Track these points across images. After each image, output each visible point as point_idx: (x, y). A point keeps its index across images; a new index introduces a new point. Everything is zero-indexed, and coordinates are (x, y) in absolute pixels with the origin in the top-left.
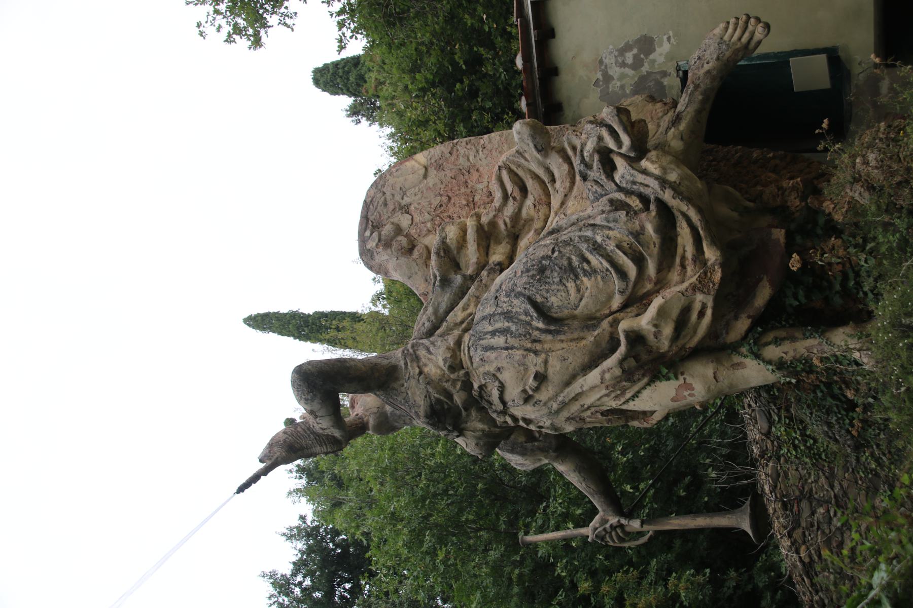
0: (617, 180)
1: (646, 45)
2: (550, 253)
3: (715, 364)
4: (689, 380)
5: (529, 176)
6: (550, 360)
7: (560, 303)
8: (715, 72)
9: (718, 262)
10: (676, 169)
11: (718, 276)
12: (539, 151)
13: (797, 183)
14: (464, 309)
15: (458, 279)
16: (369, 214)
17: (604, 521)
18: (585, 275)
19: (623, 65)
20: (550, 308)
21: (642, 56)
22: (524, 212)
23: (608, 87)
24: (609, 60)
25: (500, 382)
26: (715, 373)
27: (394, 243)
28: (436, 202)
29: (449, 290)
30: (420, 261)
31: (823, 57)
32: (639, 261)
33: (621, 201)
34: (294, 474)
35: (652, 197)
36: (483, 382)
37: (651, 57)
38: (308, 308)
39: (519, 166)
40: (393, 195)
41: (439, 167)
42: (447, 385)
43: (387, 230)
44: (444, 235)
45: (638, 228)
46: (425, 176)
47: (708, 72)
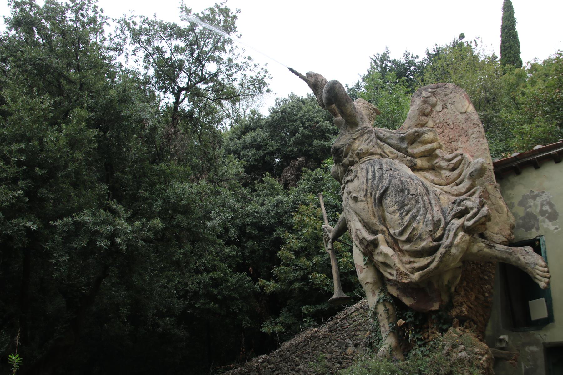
0: (453, 221)
1: (553, 217)
2: (411, 193)
3: (373, 282)
4: (364, 271)
5: (460, 171)
6: (363, 203)
7: (387, 203)
8: (519, 263)
9: (412, 280)
10: (458, 252)
11: (405, 281)
12: (470, 174)
13: (464, 312)
14: (391, 152)
15: (404, 145)
16: (440, 88)
17: (330, 231)
18: (400, 214)
19: (542, 205)
20: (385, 198)
21: (547, 215)
23: (530, 199)
24: (544, 197)
25: (354, 179)
26: (369, 283)
27: (427, 105)
28: (450, 122)
29: (399, 142)
30: (418, 121)
31: (545, 315)
32: (409, 241)
33: (440, 225)
34: (435, 47)
36: (353, 171)
37: (547, 220)
38: (518, 28)
39: (464, 165)
40: (451, 98)
41: (467, 120)
42: (350, 154)
43: (433, 100)
44: (427, 132)
45: (424, 238)
46: (461, 113)
47: (519, 259)
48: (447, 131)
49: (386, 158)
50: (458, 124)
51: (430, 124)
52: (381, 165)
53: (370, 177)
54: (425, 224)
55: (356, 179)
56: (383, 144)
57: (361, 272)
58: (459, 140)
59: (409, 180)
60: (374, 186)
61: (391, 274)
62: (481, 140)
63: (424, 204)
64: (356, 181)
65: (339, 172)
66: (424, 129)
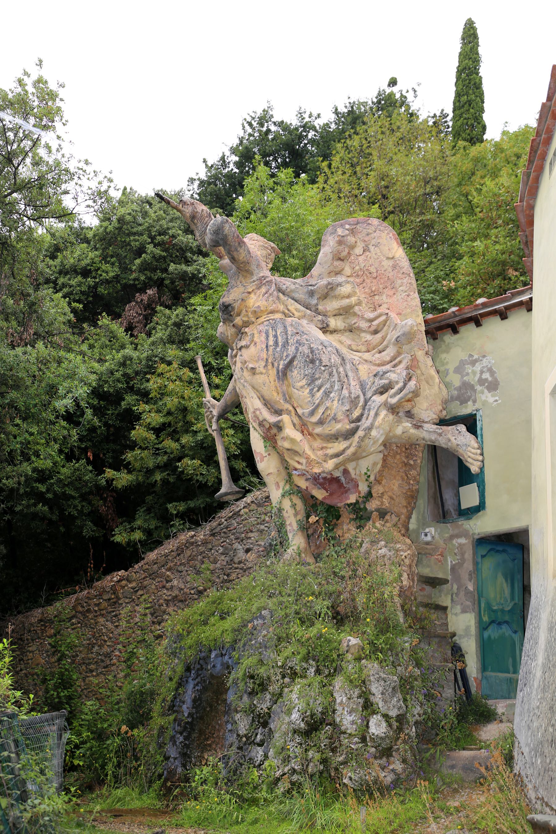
2: (324, 364)
6: (263, 376)
12: (396, 340)
14: (296, 310)
15: (314, 301)
18: (310, 390)
20: (291, 371)
22: (363, 335)
28: (372, 269)
29: (307, 297)
30: (332, 268)
32: (321, 422)
35: (359, 424)
41: (394, 267)
48: (368, 281)
49: (290, 317)
50: (383, 272)
51: (348, 271)
52: (285, 327)
53: (271, 343)
54: (340, 402)
55: (252, 345)
56: (286, 298)
57: (262, 460)
58: (383, 293)
59: (320, 347)
60: (277, 355)
61: (299, 463)
62: (412, 293)
63: (339, 377)
64: (252, 348)
65: (229, 335)
66: (340, 279)
